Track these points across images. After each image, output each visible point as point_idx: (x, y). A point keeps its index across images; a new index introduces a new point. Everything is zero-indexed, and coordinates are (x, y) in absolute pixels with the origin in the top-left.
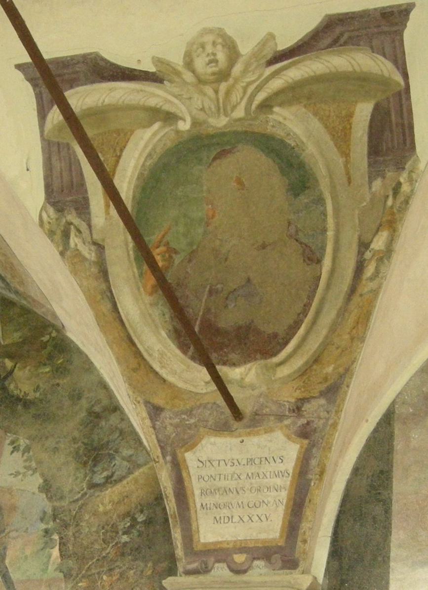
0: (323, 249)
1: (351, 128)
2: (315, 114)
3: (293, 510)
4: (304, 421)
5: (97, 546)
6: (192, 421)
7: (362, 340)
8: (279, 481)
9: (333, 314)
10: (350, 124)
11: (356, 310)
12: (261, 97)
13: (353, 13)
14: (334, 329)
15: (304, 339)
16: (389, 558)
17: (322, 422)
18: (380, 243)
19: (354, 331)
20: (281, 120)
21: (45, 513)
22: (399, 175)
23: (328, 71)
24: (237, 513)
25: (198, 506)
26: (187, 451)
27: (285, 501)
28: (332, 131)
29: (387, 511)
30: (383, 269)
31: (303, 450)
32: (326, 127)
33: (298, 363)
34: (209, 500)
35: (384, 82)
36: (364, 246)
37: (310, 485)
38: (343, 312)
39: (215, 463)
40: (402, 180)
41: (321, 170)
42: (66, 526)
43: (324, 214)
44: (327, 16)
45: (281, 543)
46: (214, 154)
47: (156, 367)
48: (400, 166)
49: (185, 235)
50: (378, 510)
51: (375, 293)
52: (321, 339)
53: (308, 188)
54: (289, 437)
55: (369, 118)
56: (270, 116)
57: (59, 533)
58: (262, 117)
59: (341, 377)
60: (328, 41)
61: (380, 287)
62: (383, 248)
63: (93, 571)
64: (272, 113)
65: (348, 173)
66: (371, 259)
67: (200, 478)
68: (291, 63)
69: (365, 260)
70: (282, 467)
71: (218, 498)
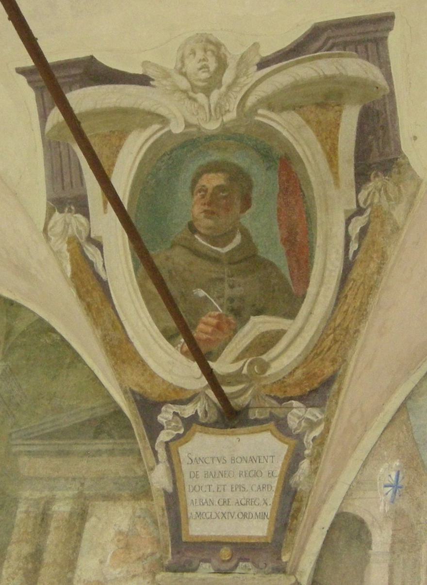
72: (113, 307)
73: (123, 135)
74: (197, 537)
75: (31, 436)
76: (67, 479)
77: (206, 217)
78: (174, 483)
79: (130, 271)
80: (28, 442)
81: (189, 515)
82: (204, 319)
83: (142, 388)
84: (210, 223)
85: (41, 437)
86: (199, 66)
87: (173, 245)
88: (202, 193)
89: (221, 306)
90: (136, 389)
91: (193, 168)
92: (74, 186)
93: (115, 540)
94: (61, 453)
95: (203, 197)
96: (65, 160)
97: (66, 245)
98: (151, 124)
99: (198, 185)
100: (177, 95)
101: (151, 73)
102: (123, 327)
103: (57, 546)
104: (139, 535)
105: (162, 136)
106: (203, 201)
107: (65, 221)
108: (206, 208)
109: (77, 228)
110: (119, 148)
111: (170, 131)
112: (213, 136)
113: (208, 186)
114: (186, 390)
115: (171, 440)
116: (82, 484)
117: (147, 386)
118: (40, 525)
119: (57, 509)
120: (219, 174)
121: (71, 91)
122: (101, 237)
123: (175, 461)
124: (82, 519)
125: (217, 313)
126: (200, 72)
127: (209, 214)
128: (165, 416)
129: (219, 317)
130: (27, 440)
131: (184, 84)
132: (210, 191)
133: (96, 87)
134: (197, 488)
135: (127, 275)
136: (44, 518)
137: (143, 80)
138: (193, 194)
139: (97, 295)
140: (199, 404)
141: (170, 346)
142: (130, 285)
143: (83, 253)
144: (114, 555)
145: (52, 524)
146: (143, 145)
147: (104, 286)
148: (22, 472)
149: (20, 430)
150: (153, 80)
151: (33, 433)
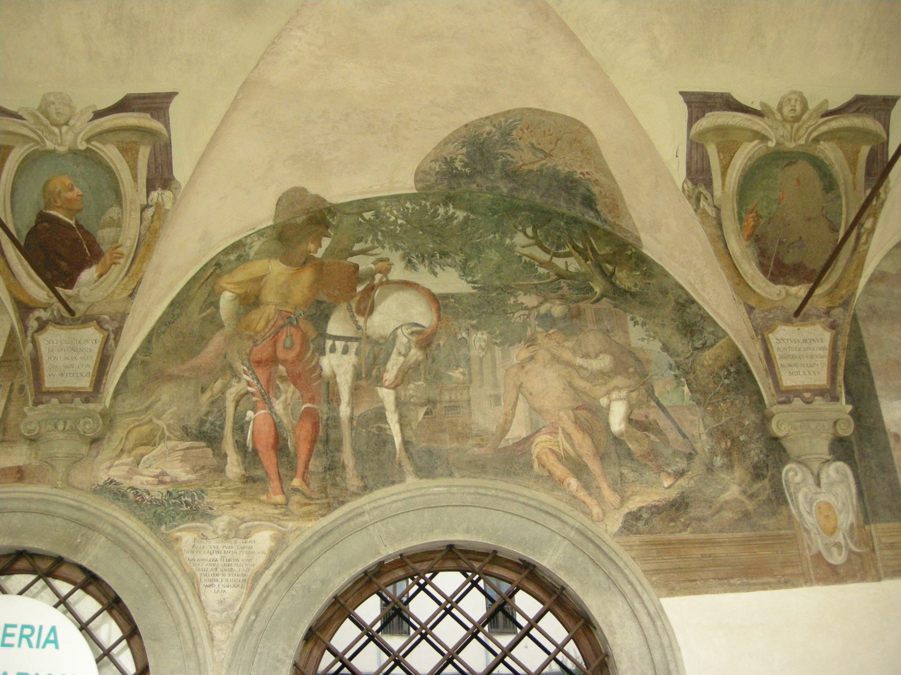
0: (840, 224)
4: (832, 320)
5: (711, 386)
6: (771, 316)
8: (822, 353)
9: (845, 262)
14: (845, 270)
21: (671, 365)
24: (802, 369)
25: (780, 365)
26: (770, 333)
32: (845, 156)
34: (785, 362)
35: (877, 136)
38: (850, 261)
39: (786, 341)
41: (841, 181)
42: (688, 373)
45: (828, 387)
46: (786, 162)
47: (750, 283)
49: (766, 208)
51: (866, 251)
53: (833, 189)
54: (825, 329)
57: (684, 377)
58: (813, 146)
63: (714, 401)
67: (778, 349)
70: (822, 345)
71: (789, 361)
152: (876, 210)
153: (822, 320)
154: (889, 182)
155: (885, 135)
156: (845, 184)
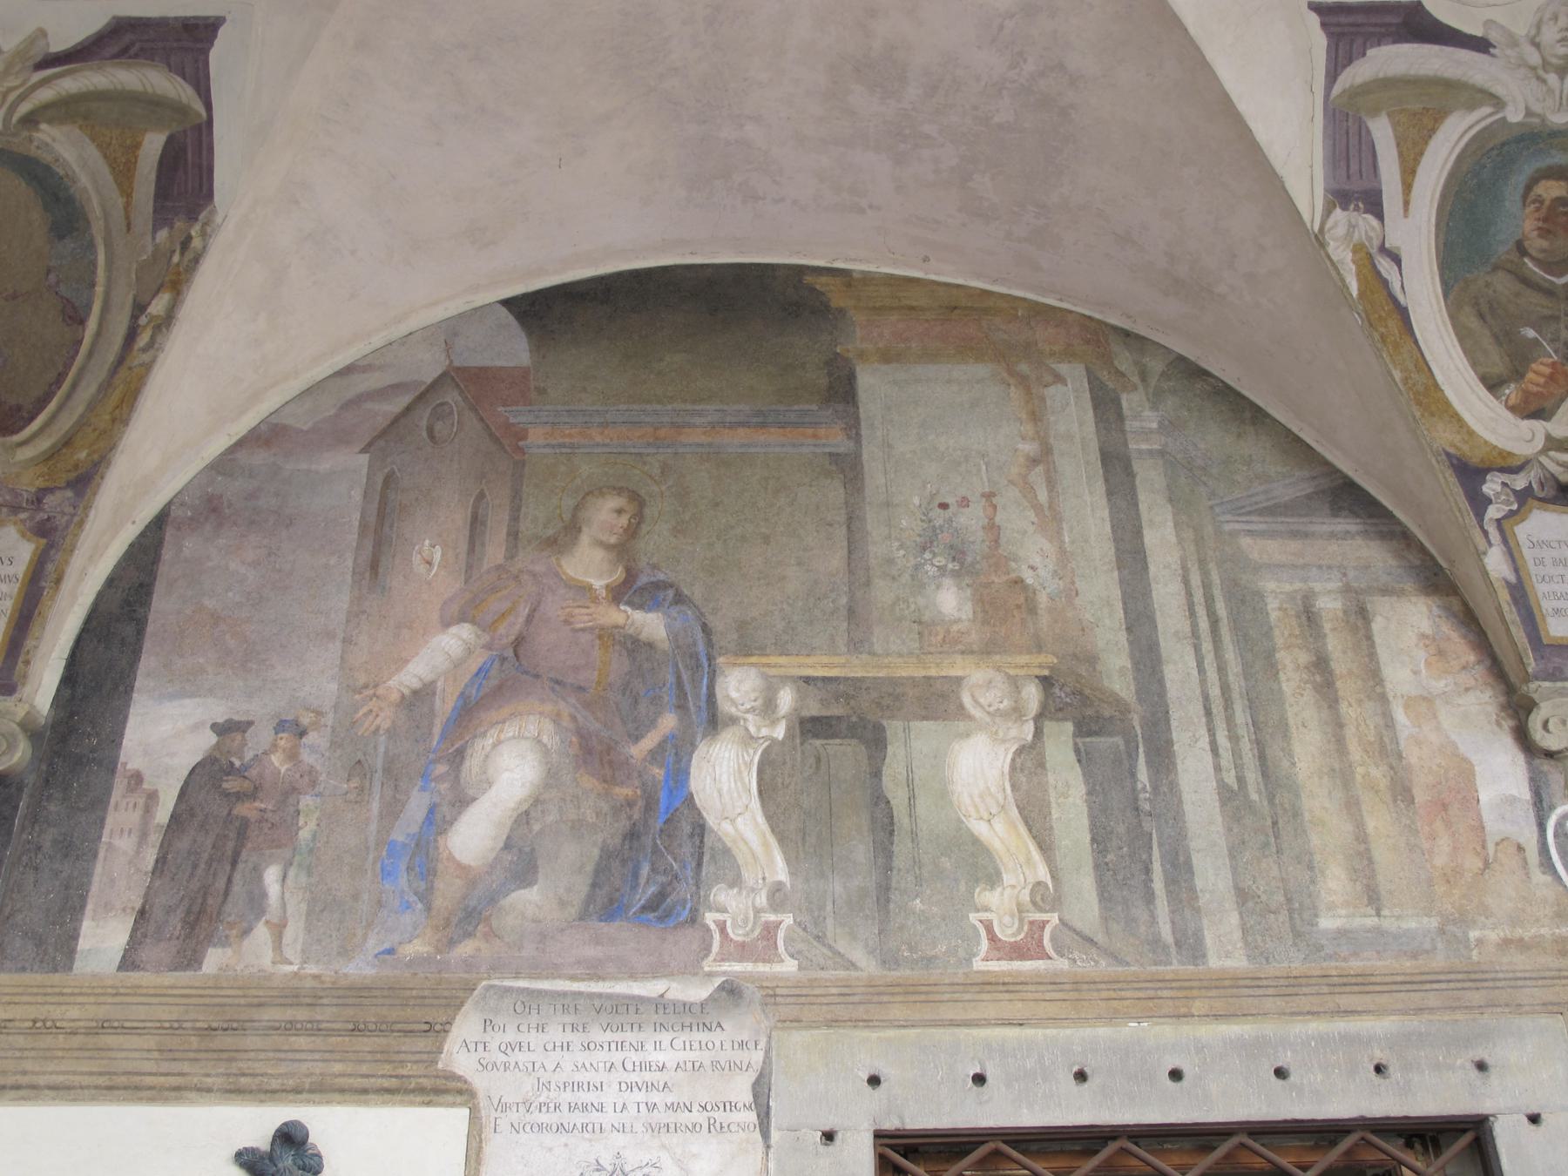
0: (89, 306)
1: (136, 162)
2: (93, 140)
3: (16, 624)
7: (126, 422)
9: (93, 389)
10: (136, 157)
11: (122, 386)
12: (24, 108)
13: (149, 19)
14: (91, 407)
15: (53, 417)
16: (132, 687)
17: (66, 518)
18: (159, 307)
19: (117, 411)
20: (49, 140)
22: (191, 226)
23: (112, 87)
27: (9, 612)
28: (112, 163)
29: (140, 632)
30: (159, 339)
31: (39, 552)
32: (105, 156)
33: (44, 444)
35: (181, 110)
36: (139, 308)
37: (42, 595)
38: (106, 386)
40: (193, 233)
41: (95, 208)
43: (94, 264)
44: (114, 18)
48: (192, 216)
50: (129, 630)
51: (148, 367)
52: (75, 417)
54: (23, 535)
55: (160, 152)
56: (35, 134)
58: (25, 134)
59: (95, 465)
60: (115, 49)
61: (153, 361)
62: (162, 313)
64: (38, 130)
65: (127, 217)
66: (145, 327)
68: (64, 71)
69: (138, 326)
70: (10, 570)
72: (1416, 342)
73: (1439, 116)
74: (1562, 638)
75: (1243, 511)
76: (1320, 567)
77: (1540, 236)
78: (1516, 570)
79: (1437, 297)
80: (1244, 519)
81: (1544, 611)
82: (1533, 366)
83: (1457, 448)
84: (1544, 244)
85: (1261, 512)
86: (1559, 36)
87: (1496, 268)
88: (1537, 205)
89: (1556, 352)
90: (1452, 451)
91: (1529, 169)
92: (1364, 175)
93: (1421, 645)
94: (1294, 535)
95: (1538, 210)
96: (1354, 141)
97: (1351, 254)
98: (1481, 105)
99: (1532, 193)
100: (1523, 71)
101: (1493, 36)
102: (1430, 369)
103: (1344, 652)
104: (1449, 639)
105: (1492, 124)
106: (1537, 215)
107: (1350, 221)
108: (1540, 224)
109: (1366, 232)
110: (1433, 131)
111: (1504, 119)
112: (1560, 132)
113: (1545, 195)
114: (1514, 455)
115: (1503, 518)
116: (1345, 575)
117: (1465, 448)
118: (1309, 626)
119: (1322, 605)
120: (1562, 183)
121: (1379, 45)
122: (1398, 248)
123: (1512, 544)
124: (1364, 618)
125: (1550, 360)
126: (1559, 45)
127: (1544, 233)
128: (1492, 486)
129: (1554, 364)
130: (1239, 515)
131: (1534, 58)
132: (1547, 203)
133: (1415, 45)
134: (1547, 578)
135: (1434, 301)
136: (1309, 617)
137: (1481, 45)
138: (1524, 205)
139: (1394, 325)
140: (1532, 474)
141: (1492, 398)
142: (1438, 316)
143: (1374, 266)
144: (1428, 664)
145: (1325, 625)
146: (1466, 132)
147: (1403, 314)
148: (1250, 557)
149: (1222, 503)
150: (1494, 47)
151: (1243, 507)
152: (179, 273)
153: (23, 516)
154: (213, 212)
155: (199, 106)
156: (106, 215)
